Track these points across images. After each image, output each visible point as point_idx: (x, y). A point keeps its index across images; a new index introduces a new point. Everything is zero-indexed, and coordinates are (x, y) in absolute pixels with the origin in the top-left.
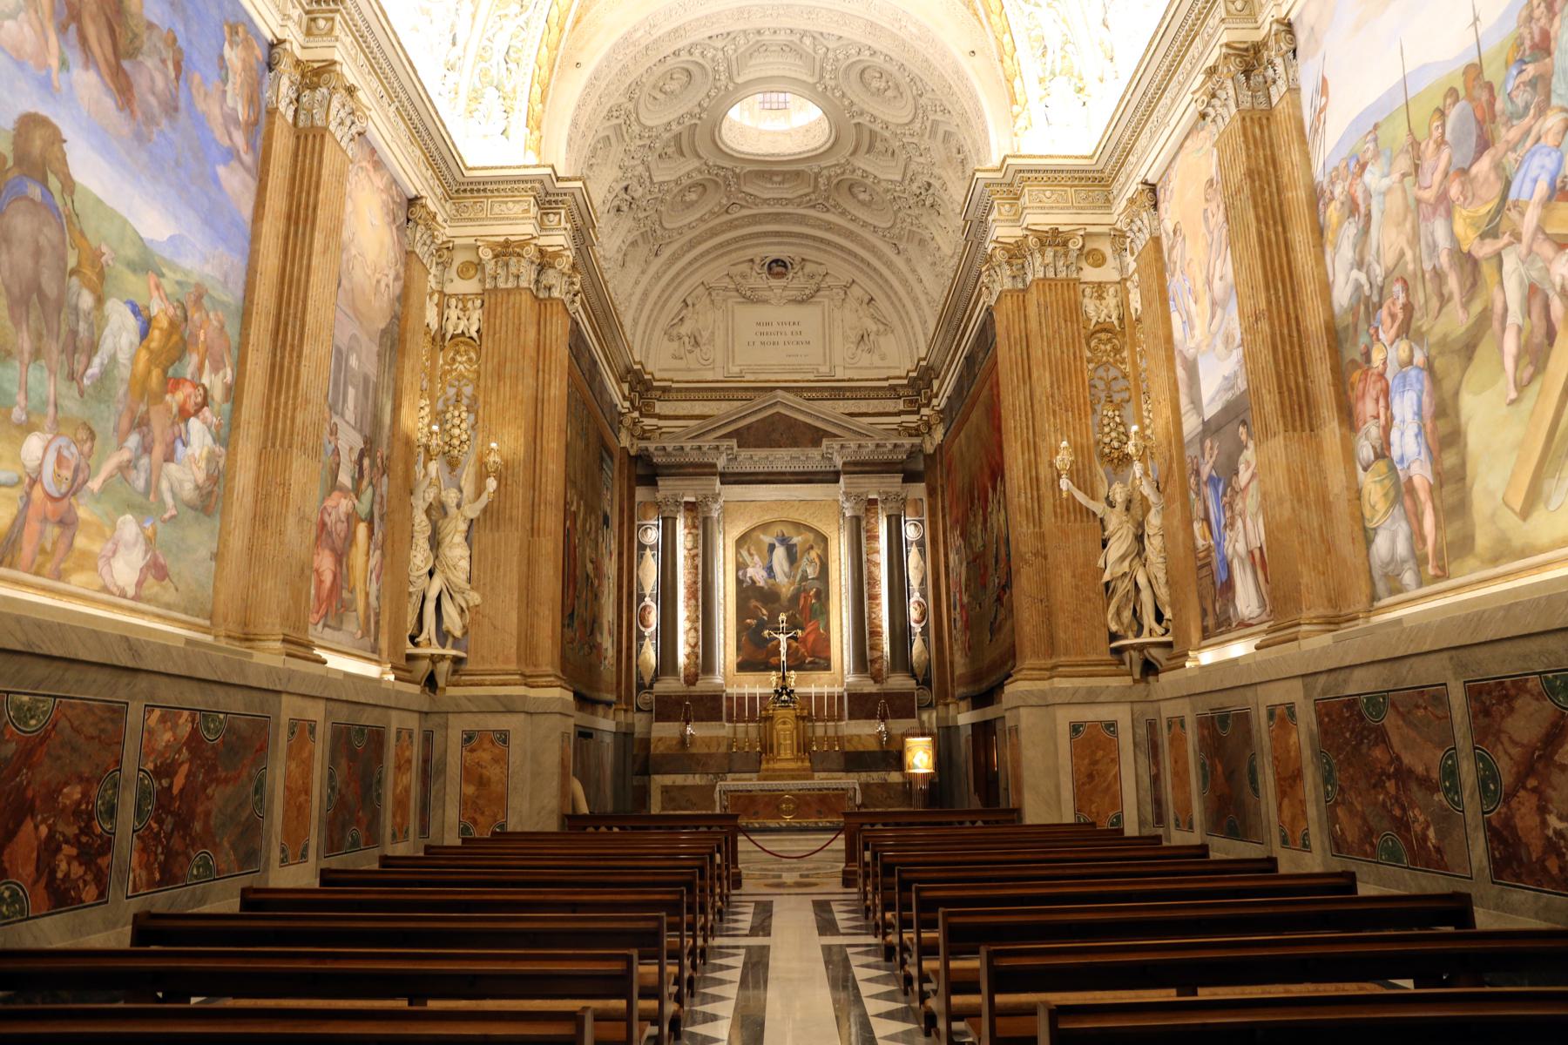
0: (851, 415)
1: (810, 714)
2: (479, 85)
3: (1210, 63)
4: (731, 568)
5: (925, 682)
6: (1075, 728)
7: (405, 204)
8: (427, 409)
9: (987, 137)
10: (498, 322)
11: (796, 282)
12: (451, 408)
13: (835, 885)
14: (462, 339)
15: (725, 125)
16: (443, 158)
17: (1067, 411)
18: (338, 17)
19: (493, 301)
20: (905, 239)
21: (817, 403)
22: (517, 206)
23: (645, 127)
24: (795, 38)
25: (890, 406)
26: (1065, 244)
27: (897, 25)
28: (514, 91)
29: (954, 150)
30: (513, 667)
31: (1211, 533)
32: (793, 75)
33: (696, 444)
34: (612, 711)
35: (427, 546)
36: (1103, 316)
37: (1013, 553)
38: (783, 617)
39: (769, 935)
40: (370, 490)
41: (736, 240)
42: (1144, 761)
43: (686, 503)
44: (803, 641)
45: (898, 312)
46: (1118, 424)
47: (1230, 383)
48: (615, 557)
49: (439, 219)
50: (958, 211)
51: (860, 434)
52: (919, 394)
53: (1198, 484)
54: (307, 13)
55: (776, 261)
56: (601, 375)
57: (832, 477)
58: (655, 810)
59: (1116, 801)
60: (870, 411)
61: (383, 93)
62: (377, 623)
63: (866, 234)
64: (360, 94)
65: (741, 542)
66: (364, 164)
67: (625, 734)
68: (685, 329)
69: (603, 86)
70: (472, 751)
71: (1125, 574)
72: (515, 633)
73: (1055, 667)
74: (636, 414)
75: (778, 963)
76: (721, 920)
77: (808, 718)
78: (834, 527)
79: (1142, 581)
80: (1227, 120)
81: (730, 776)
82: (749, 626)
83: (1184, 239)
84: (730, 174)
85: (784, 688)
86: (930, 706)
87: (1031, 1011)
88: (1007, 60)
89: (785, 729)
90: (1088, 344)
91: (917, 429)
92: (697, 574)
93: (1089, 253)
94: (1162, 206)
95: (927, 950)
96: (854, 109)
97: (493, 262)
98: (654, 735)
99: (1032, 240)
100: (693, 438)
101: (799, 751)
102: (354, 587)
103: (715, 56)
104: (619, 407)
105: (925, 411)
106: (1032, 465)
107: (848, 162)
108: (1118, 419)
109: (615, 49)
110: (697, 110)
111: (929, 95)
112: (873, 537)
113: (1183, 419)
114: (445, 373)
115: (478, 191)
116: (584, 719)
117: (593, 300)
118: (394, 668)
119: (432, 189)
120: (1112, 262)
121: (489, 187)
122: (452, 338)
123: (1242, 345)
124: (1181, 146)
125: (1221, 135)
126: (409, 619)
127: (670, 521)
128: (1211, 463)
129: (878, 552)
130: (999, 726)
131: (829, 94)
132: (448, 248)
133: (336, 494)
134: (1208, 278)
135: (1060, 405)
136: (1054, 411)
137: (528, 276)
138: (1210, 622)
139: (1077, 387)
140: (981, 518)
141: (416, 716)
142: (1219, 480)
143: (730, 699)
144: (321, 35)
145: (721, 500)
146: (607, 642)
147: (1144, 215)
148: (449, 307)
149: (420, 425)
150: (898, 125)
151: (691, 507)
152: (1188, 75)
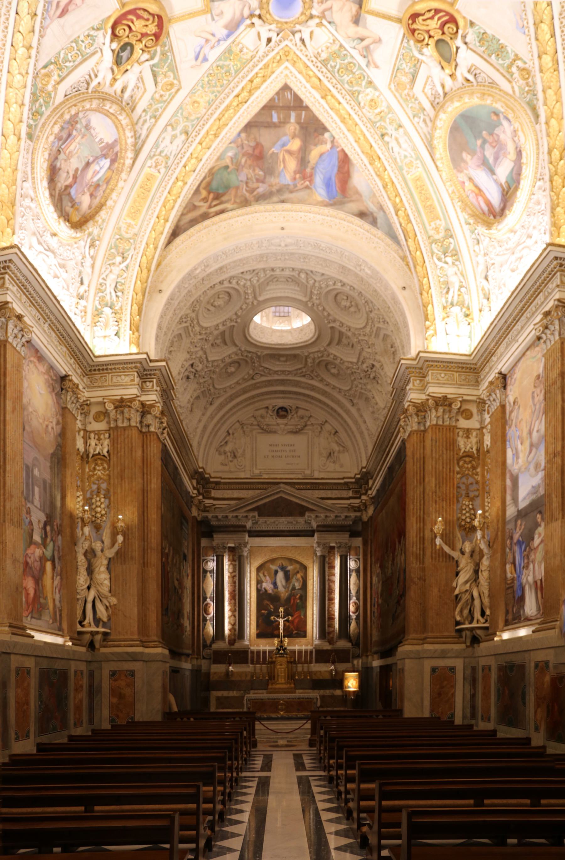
0: (323, 499)
1: (295, 660)
3: (547, 309)
4: (254, 582)
5: (356, 644)
6: (434, 670)
7: (59, 380)
8: (81, 497)
10: (119, 446)
11: (292, 421)
12: (95, 496)
13: (305, 746)
14: (99, 457)
15: (252, 326)
17: (443, 500)
19: (115, 434)
20: (357, 397)
21: (303, 491)
23: (202, 327)
24: (295, 274)
25: (344, 494)
26: (450, 405)
27: (358, 268)
30: (136, 637)
31: (515, 570)
32: (293, 296)
33: (235, 514)
34: (189, 659)
35: (85, 573)
36: (468, 448)
37: (407, 577)
38: (281, 609)
39: (270, 771)
40: (51, 544)
41: (258, 395)
42: (468, 687)
43: (230, 547)
44: (292, 622)
45: (351, 439)
46: (470, 509)
47: (535, 489)
48: (190, 577)
51: (326, 509)
52: (361, 488)
53: (511, 544)
55: (282, 408)
56: (180, 475)
57: (310, 533)
58: (213, 709)
59: (452, 707)
60: (333, 497)
62: (61, 615)
63: (335, 393)
65: (259, 569)
66: (32, 359)
67: (197, 670)
68: (228, 448)
69: (176, 303)
70: (115, 680)
71: (467, 591)
72: (136, 619)
73: (425, 638)
74: (201, 497)
75: (274, 785)
76: (246, 764)
77: (294, 662)
78: (311, 561)
79: (475, 594)
80: (553, 343)
81: (252, 691)
82: (263, 614)
83: (519, 407)
84: (254, 356)
85: (281, 647)
86: (358, 657)
87: (398, 810)
88: (425, 293)
89: (281, 668)
90: (458, 464)
91: (359, 507)
92: (235, 586)
93: (463, 411)
95: (350, 780)
98: (212, 671)
99: (431, 402)
100: (233, 511)
101: (288, 679)
102: (47, 597)
103: (245, 284)
104: (191, 493)
105: (364, 497)
106: (421, 530)
107: (325, 350)
108: (471, 506)
109: (183, 281)
111: (376, 312)
112: (333, 567)
113: (507, 508)
114: (90, 476)
116: (175, 663)
117: (174, 432)
118: (71, 639)
119: (75, 370)
120: (476, 417)
121: (109, 367)
122: (93, 456)
123: (544, 469)
124: (524, 354)
126: (78, 612)
127: (220, 557)
128: (520, 533)
129: (334, 575)
130: (394, 668)
131: (315, 308)
133: (33, 547)
134: (530, 430)
135: (439, 497)
136: (436, 501)
138: (510, 617)
139: (450, 488)
140: (391, 558)
141: (85, 663)
142: (523, 542)
143: (252, 652)
145: (249, 546)
146: (187, 624)
147: (498, 392)
149: (78, 506)
150: (356, 329)
151: (232, 550)
152: (533, 314)
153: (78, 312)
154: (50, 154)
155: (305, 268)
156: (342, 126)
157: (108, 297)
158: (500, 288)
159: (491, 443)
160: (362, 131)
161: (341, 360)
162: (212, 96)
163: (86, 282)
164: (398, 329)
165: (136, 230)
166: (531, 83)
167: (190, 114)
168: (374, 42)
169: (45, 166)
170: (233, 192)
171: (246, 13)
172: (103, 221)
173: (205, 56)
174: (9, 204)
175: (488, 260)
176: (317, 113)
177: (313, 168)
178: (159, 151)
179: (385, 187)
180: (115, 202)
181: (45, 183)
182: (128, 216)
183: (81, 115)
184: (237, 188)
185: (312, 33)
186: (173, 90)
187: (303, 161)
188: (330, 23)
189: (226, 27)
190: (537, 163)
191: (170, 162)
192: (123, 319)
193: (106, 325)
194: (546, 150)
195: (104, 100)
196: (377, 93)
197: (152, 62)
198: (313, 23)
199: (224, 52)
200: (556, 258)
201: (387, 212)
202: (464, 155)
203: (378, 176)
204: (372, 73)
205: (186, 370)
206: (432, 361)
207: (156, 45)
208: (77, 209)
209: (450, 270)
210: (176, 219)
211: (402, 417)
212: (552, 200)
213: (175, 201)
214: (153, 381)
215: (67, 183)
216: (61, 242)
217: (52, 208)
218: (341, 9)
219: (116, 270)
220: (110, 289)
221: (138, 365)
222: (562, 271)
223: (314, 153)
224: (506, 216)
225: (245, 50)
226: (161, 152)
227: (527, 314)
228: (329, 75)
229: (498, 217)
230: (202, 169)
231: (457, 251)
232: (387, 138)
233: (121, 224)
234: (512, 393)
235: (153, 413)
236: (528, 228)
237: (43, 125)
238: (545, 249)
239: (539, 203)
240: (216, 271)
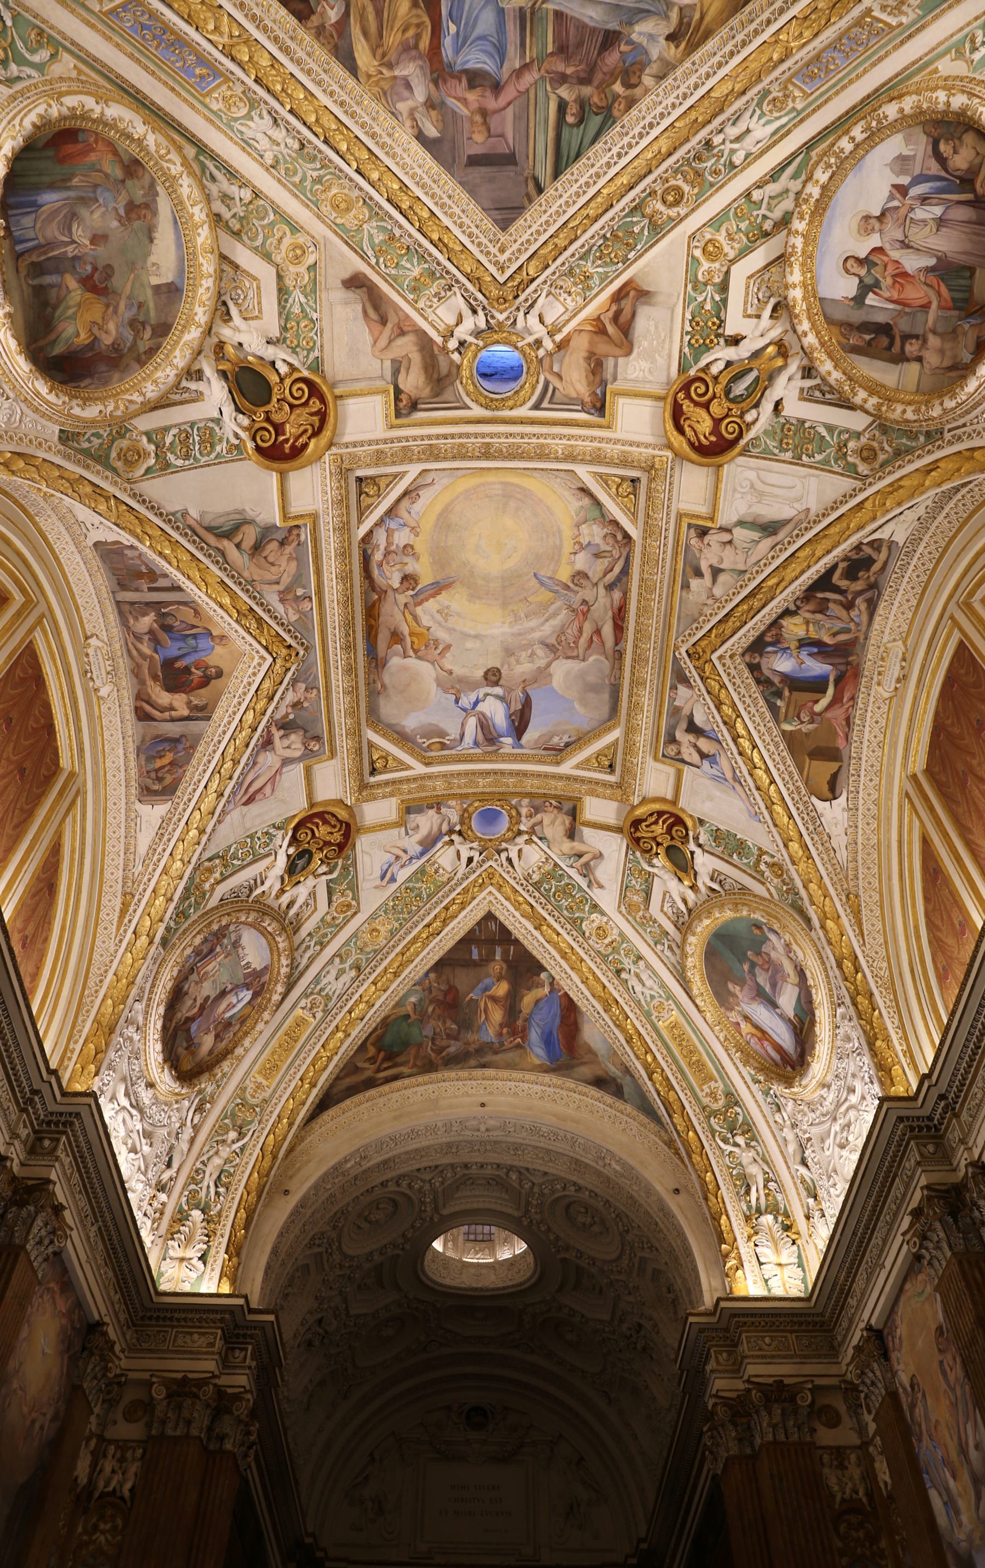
2: (186, 1208)
3: (914, 1204)
9: (697, 1277)
16: (135, 1282)
18: (64, 1138)
22: (203, 1339)
24: (502, 1173)
26: (792, 1399)
27: (601, 1163)
28: (219, 1214)
29: (664, 1289)
32: (499, 1208)
36: (848, 1491)
49: (117, 1348)
50: (673, 1356)
54: (35, 1132)
61: (89, 1212)
64: (66, 1214)
69: (309, 1213)
80: (944, 1264)
83: (924, 1395)
94: (894, 1356)
96: (560, 1243)
97: (165, 1403)
103: (421, 1188)
109: (324, 1178)
110: (401, 1241)
115: (165, 1319)
119: (116, 1314)
120: (848, 1421)
122: (103, 1495)
124: (901, 1290)
125: (941, 1279)
132: (120, 1383)
134: (960, 1444)
137: (201, 1418)
144: (43, 1154)
147: (875, 1365)
148: (105, 1456)
152: (895, 1215)
153: (150, 1211)
154: (180, 971)
155: (516, 1163)
156: (563, 963)
157: (203, 1194)
158: (829, 1177)
159: (891, 1477)
160: (590, 968)
161: (583, 1316)
162: (397, 925)
163: (175, 1165)
164: (676, 1259)
165: (266, 1094)
166: (787, 880)
167: (366, 944)
168: (594, 858)
169: (169, 985)
170: (413, 1051)
171: (445, 828)
172: (224, 1075)
173: (393, 875)
174: (107, 1030)
175: (800, 1134)
176: (530, 948)
177: (526, 1020)
178: (318, 987)
179: (629, 1041)
180: (246, 1051)
181: (162, 1010)
182: (260, 1072)
183: (232, 928)
184: (420, 1045)
185: (520, 851)
186: (349, 913)
187: (511, 1005)
188: (541, 839)
189: (421, 843)
190: (829, 983)
191: (330, 1005)
192: (219, 1233)
193: (189, 1240)
194: (834, 965)
195: (264, 914)
196: (605, 919)
197: (329, 877)
198: (521, 840)
199: (416, 873)
200: (900, 1119)
201: (637, 1076)
202: (730, 986)
203: (618, 1026)
204: (597, 895)
205: (309, 1329)
206: (744, 1315)
207: (338, 857)
208: (193, 1054)
209: (746, 1157)
210: (328, 1084)
211: (705, 1429)
212: (864, 1032)
213: (330, 1059)
214: (246, 1349)
215: (190, 1014)
216: (156, 1098)
217: (159, 1047)
218: (553, 823)
219: (225, 1152)
220: (209, 1181)
221: (227, 1316)
222: (916, 1137)
223: (528, 1000)
224: (809, 1065)
225: (441, 871)
226: (321, 990)
227: (885, 1217)
228: (543, 900)
229: (798, 1068)
230: (373, 1017)
231: (749, 1125)
232: (624, 975)
233: (247, 1082)
234: (901, 1367)
235: (236, 1413)
236: (845, 1077)
237: (184, 933)
238: (880, 1108)
239: (848, 1039)
240: (378, 1165)
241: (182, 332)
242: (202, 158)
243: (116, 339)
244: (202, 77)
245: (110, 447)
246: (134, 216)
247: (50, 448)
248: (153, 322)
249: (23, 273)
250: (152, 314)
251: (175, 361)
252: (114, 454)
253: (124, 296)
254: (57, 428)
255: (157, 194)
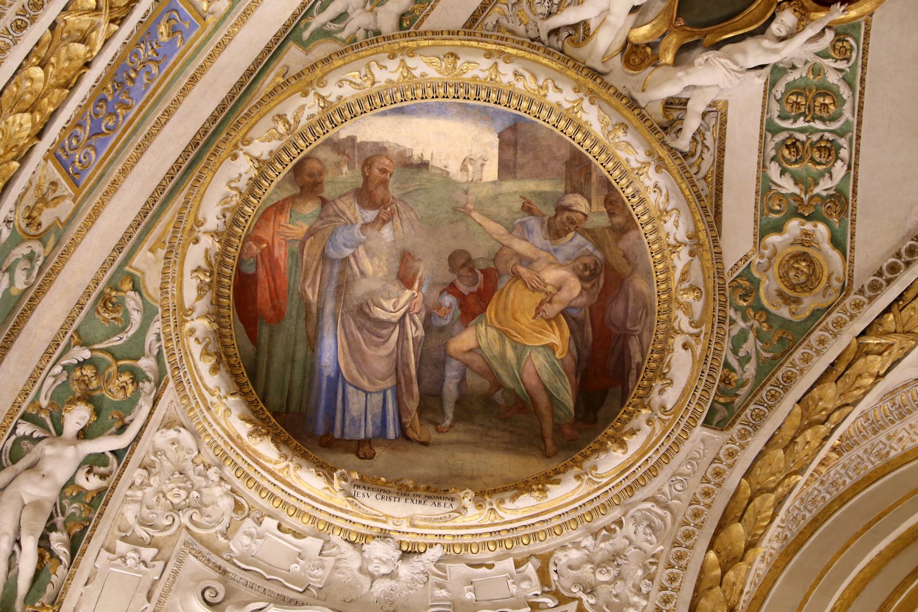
241: (587, 135)
242: (306, 35)
243: (574, 270)
244: (173, 31)
245: (770, 317)
246: (379, 193)
247: (731, 454)
248: (561, 189)
249: (430, 433)
250: (546, 186)
251: (634, 164)
252: (784, 312)
253: (506, 240)
254: (700, 432)
255: (352, 139)
